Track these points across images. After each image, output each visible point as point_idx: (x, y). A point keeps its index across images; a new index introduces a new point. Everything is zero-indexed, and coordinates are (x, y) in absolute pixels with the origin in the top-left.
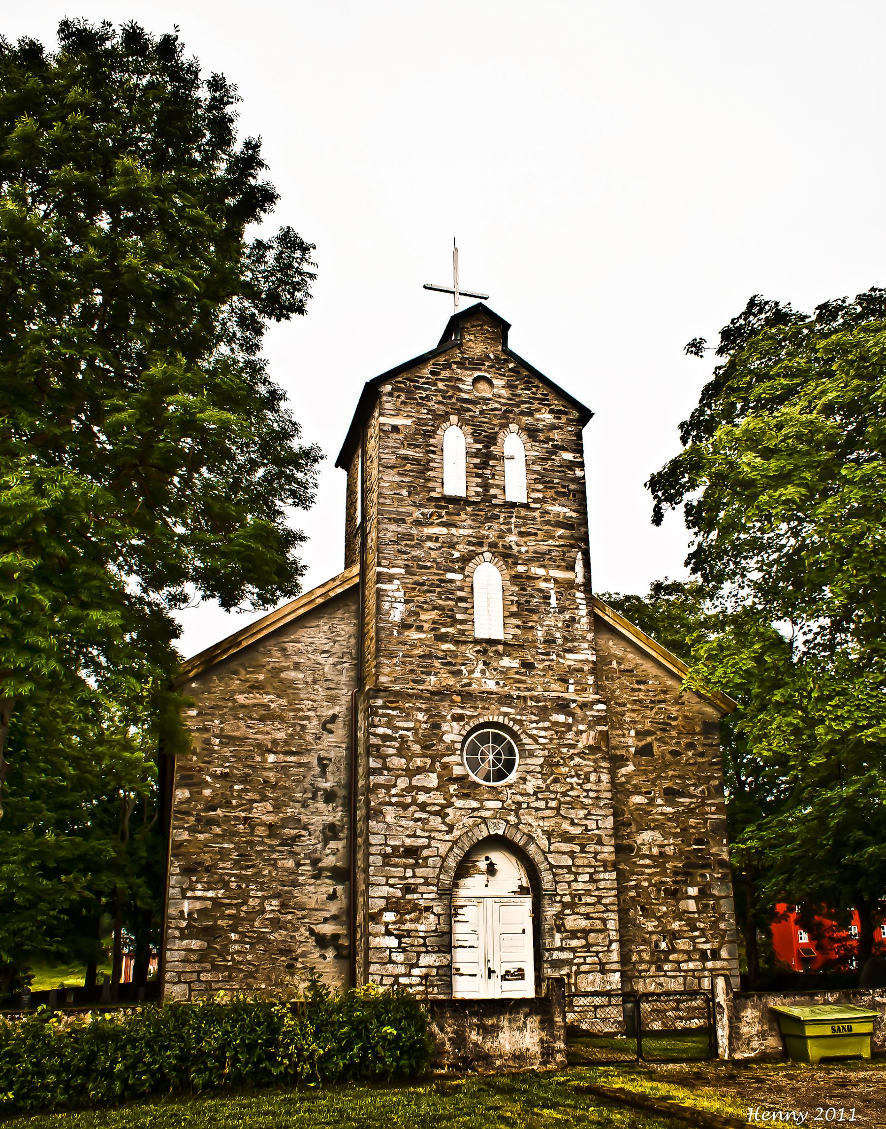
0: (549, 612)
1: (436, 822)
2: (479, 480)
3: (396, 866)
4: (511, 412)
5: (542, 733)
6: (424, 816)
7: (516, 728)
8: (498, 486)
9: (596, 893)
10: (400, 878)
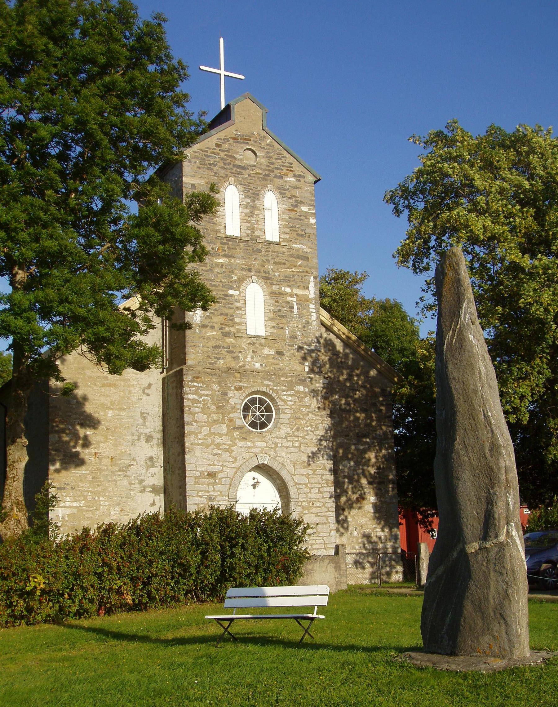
0: (293, 318)
1: (226, 455)
2: (248, 225)
3: (203, 484)
4: (268, 175)
5: (290, 398)
6: (219, 452)
7: (274, 395)
8: (260, 230)
9: (322, 500)
10: (206, 492)
